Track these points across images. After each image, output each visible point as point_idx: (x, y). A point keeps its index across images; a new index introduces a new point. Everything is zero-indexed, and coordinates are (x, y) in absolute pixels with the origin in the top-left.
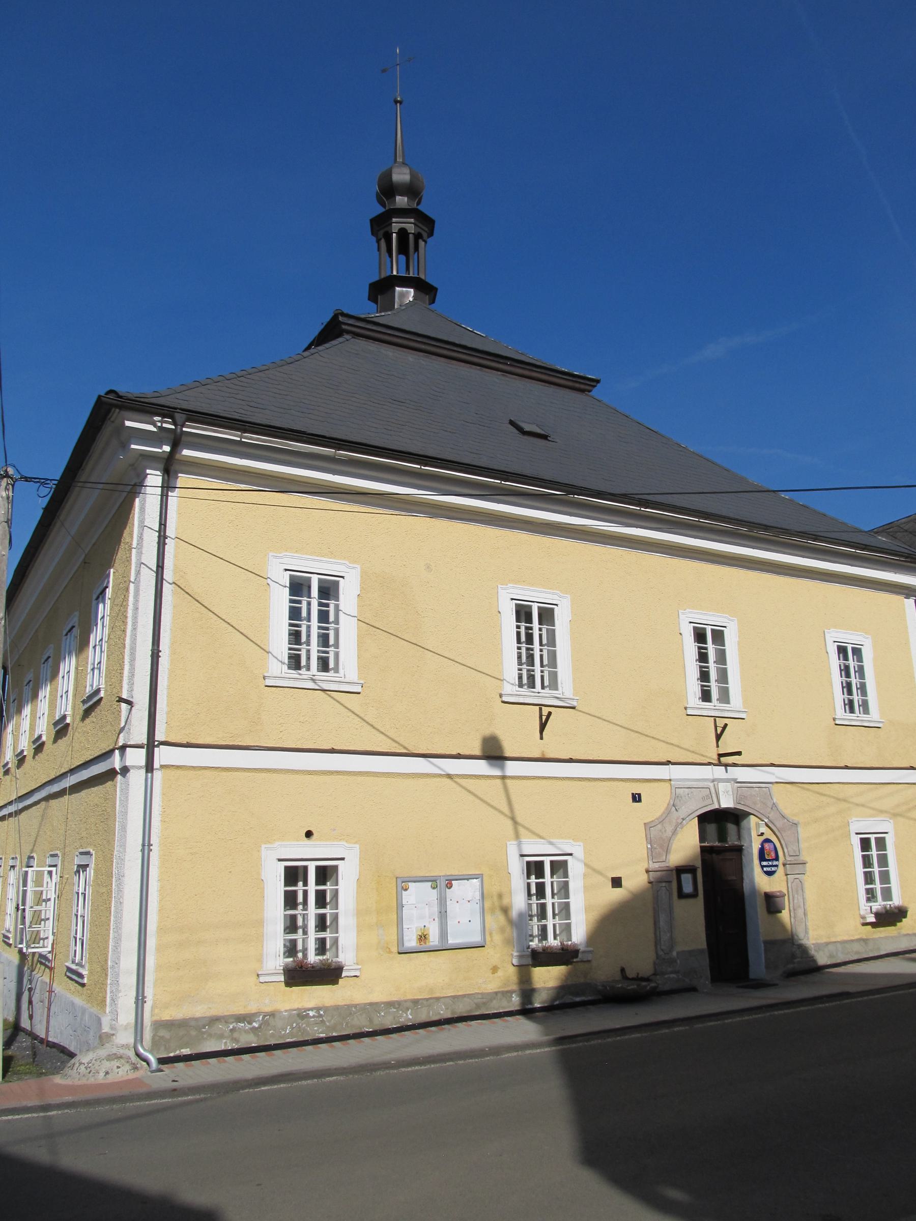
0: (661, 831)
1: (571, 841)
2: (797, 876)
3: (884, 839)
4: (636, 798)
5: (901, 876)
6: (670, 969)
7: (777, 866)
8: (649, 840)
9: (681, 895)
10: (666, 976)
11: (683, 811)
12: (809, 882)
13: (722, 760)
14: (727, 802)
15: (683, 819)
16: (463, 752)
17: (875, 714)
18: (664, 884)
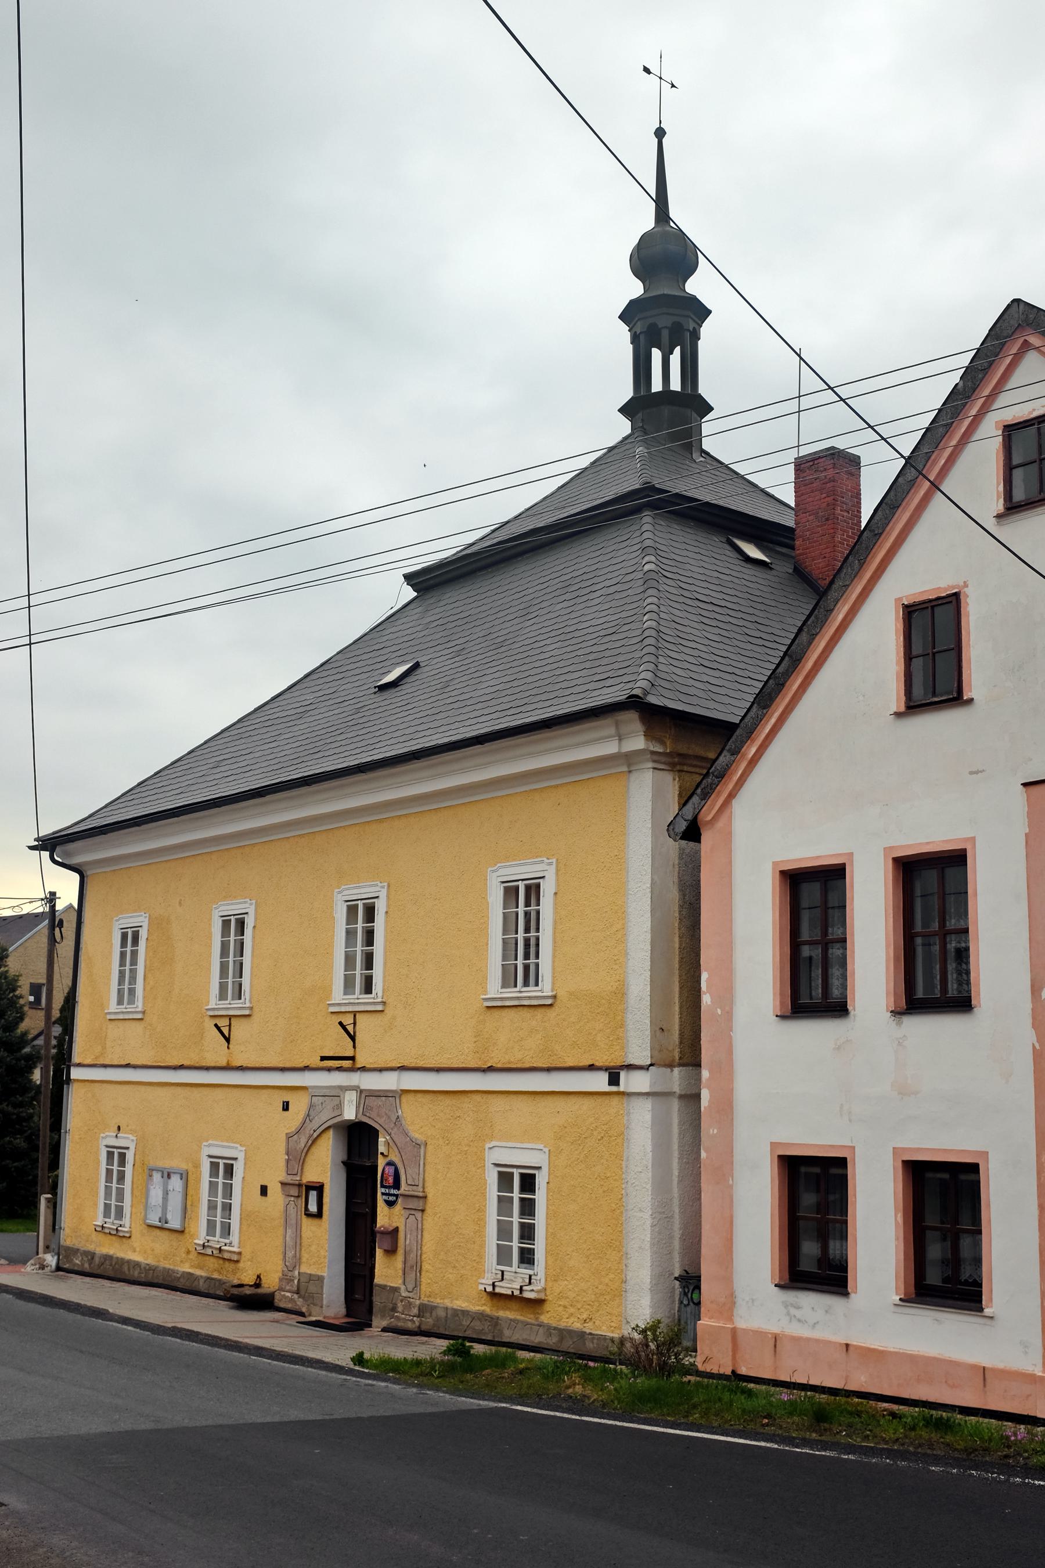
0: (296, 1141)
1: (238, 1146)
2: (413, 1212)
3: (533, 1176)
4: (286, 1107)
5: (550, 1236)
6: (288, 1288)
7: (397, 1196)
8: (287, 1154)
9: (308, 1215)
10: (283, 1293)
11: (315, 1124)
12: (430, 1222)
13: (348, 1063)
14: (350, 1114)
15: (315, 1131)
16: (186, 1063)
17: (546, 987)
18: (292, 1199)
